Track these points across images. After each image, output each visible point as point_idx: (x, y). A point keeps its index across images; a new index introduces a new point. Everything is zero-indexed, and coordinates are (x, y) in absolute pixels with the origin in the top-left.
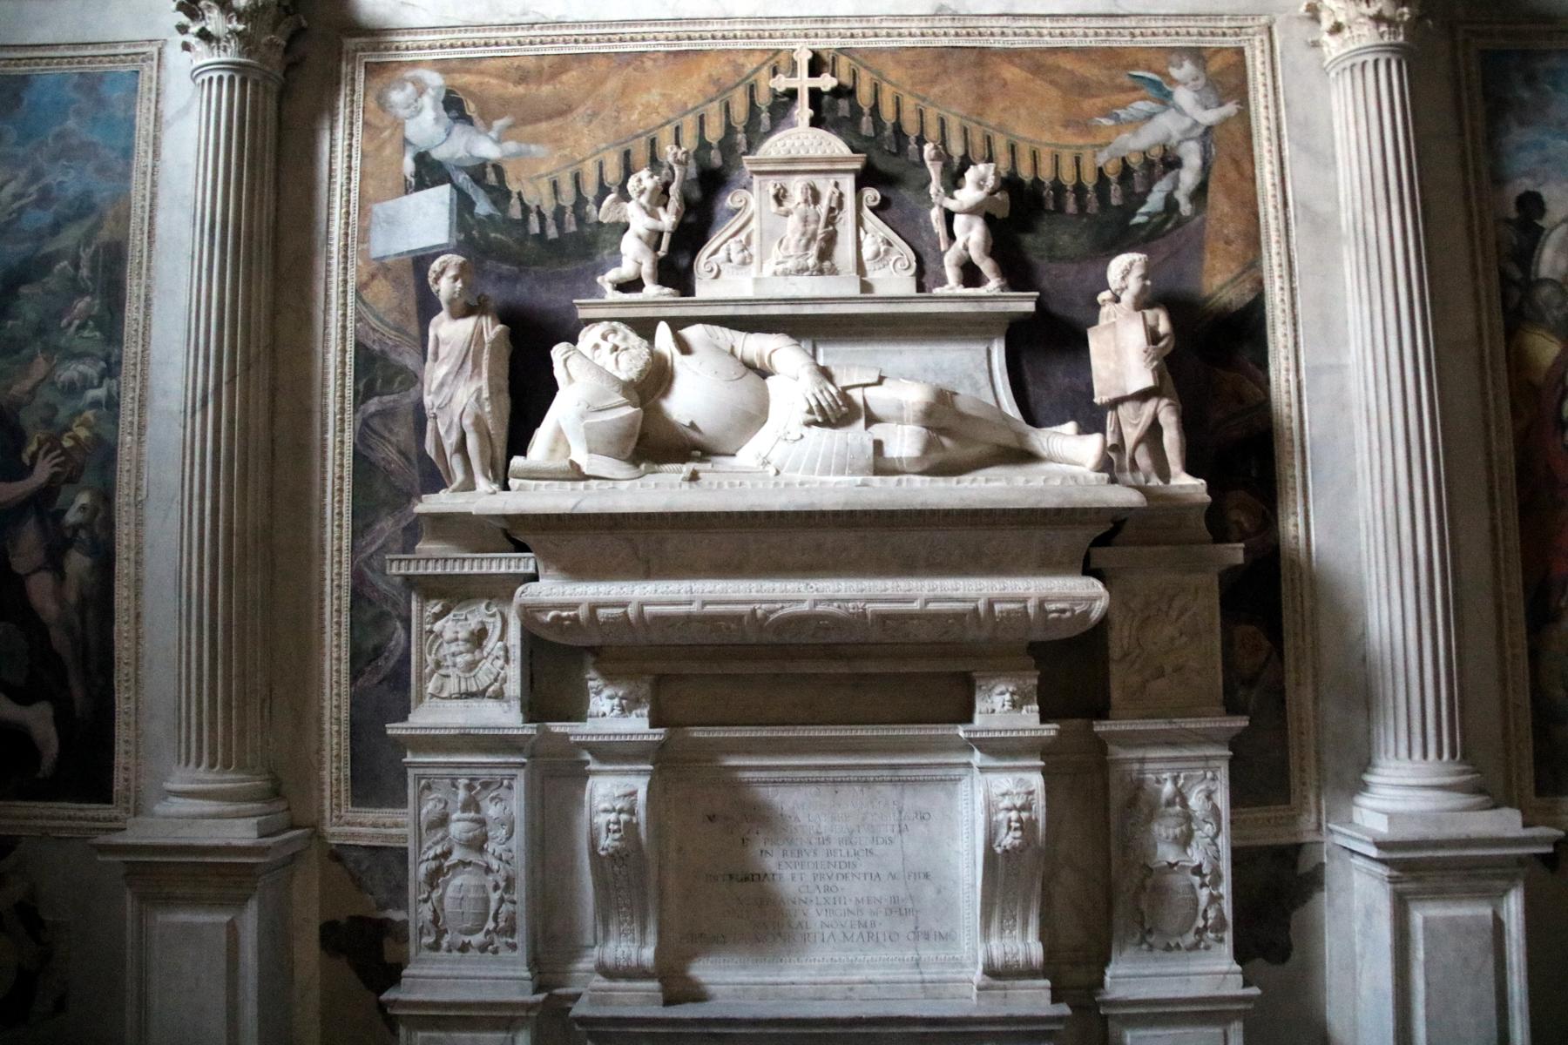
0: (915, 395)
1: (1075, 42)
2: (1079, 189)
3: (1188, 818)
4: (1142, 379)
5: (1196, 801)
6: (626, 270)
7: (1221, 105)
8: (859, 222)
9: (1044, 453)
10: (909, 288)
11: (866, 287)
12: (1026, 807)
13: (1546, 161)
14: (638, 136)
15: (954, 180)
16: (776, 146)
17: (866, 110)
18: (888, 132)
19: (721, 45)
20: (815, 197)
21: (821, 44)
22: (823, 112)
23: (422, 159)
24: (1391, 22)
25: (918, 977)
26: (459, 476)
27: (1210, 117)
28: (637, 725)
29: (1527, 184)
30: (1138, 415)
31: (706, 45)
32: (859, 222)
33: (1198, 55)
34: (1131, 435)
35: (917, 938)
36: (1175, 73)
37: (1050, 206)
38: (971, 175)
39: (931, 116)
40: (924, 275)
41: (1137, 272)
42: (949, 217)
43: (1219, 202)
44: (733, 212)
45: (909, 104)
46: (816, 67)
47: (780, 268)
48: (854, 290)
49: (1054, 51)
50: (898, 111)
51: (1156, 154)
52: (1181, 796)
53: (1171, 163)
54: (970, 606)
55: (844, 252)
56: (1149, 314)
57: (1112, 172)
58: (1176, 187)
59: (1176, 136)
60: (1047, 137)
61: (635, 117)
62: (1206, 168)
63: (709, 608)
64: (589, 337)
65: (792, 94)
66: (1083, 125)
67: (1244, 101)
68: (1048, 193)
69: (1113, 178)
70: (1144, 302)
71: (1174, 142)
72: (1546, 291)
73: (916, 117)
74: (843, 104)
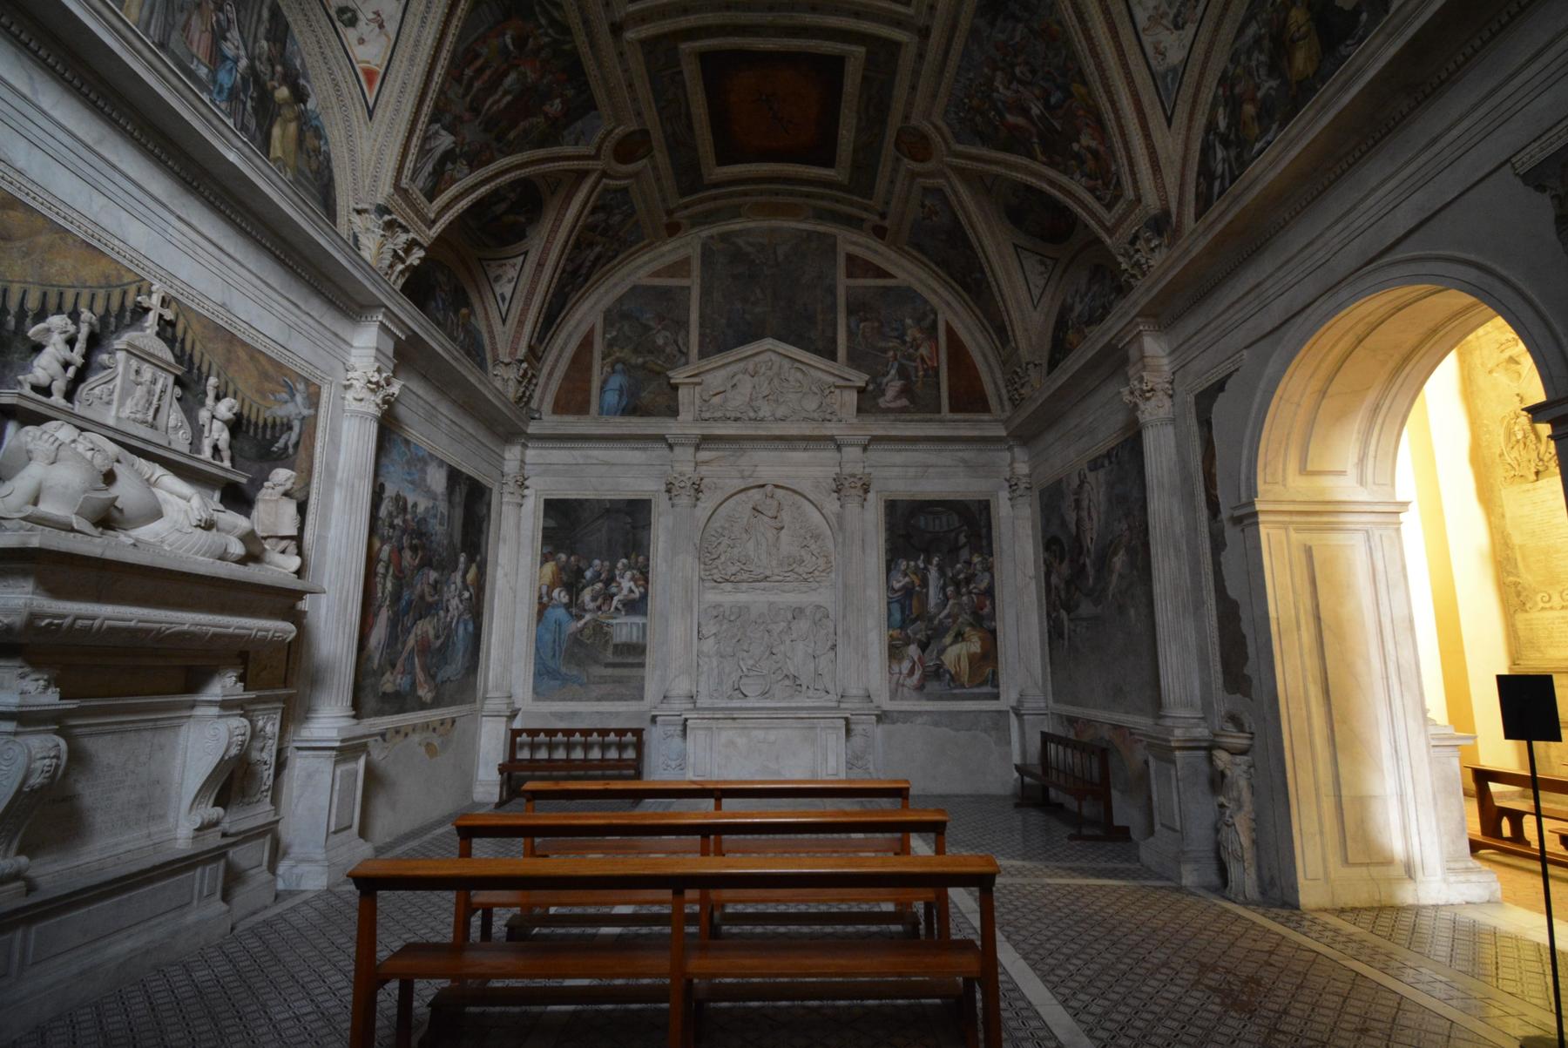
1: (269, 353)
2: (256, 424)
3: (264, 738)
5: (269, 728)
7: (309, 408)
8: (171, 405)
9: (268, 560)
10: (186, 450)
12: (244, 734)
14: (52, 286)
16: (128, 336)
17: (179, 339)
18: (186, 357)
19: (115, 256)
20: (154, 382)
22: (166, 330)
25: (151, 843)
30: (277, 545)
31: (107, 250)
32: (171, 405)
33: (307, 381)
35: (149, 821)
37: (244, 429)
39: (207, 357)
40: (195, 444)
41: (292, 480)
44: (105, 368)
45: (198, 347)
47: (133, 416)
49: (261, 352)
50: (193, 348)
51: (285, 420)
52: (263, 729)
53: (290, 428)
54: (249, 632)
57: (270, 420)
58: (288, 440)
59: (293, 416)
60: (249, 394)
61: (53, 271)
62: (300, 435)
63: (140, 625)
66: (262, 393)
67: (317, 411)
68: (245, 422)
73: (199, 354)
74: (169, 329)
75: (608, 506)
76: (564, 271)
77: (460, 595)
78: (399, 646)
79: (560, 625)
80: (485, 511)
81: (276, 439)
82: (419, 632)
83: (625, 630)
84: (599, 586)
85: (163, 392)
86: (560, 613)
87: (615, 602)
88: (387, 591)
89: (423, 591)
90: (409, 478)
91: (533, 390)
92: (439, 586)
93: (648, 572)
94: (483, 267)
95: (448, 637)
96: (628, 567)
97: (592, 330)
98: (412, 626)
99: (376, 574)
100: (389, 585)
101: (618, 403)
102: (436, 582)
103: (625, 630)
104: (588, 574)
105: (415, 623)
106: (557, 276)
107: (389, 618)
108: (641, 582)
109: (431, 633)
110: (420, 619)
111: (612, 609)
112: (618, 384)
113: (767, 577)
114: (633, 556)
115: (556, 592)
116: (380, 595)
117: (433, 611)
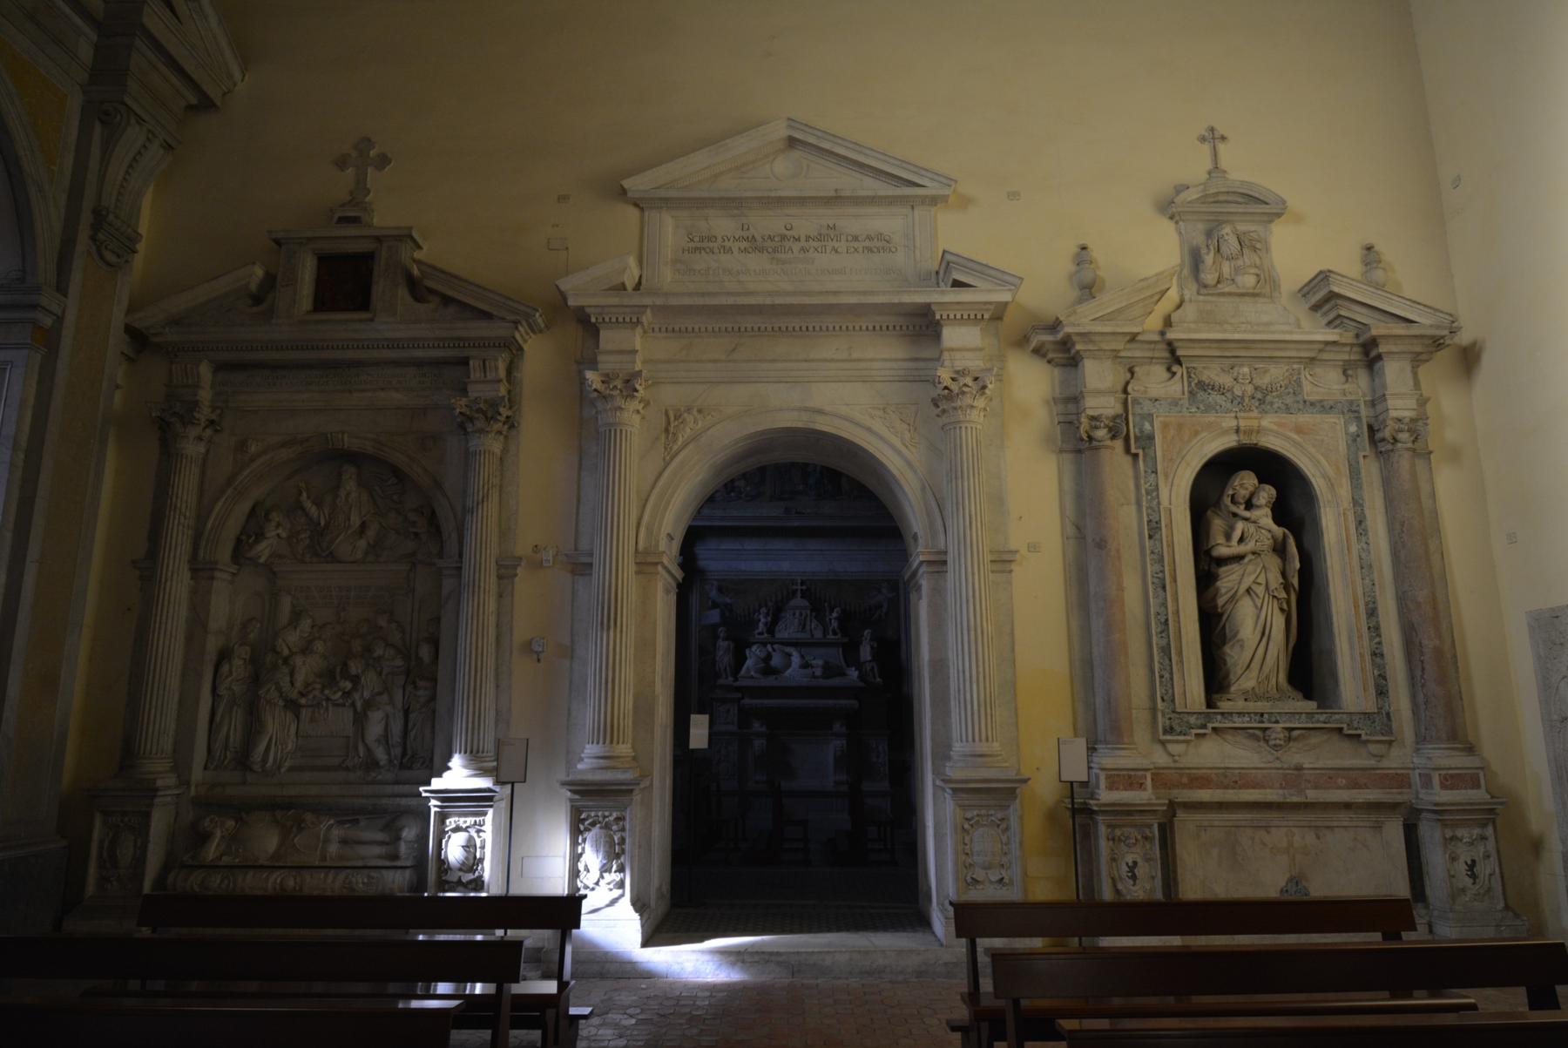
0: (820, 662)
4: (869, 658)
6: (760, 630)
11: (812, 636)
15: (832, 611)
16: (793, 603)
20: (801, 614)
21: (804, 578)
23: (713, 602)
26: (724, 676)
28: (763, 729)
34: (868, 669)
38: (835, 610)
40: (825, 632)
42: (830, 620)
46: (802, 584)
48: (809, 636)
55: (808, 628)
64: (754, 648)
65: (797, 590)
70: (871, 640)
85: (805, 618)
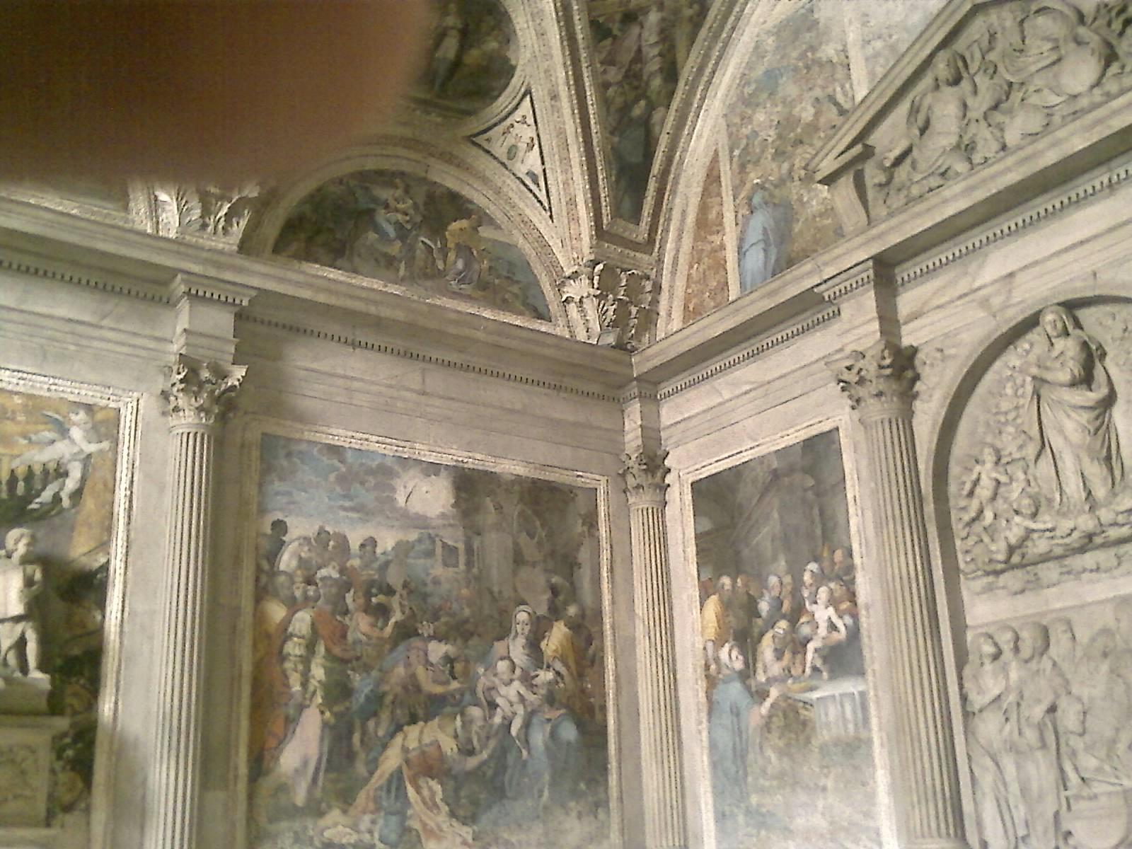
13: (293, 503)
24: (207, 412)
27: (92, 448)
29: (279, 516)
36: (73, 417)
41: (24, 541)
43: (89, 503)
51: (52, 466)
53: (62, 473)
56: (29, 568)
57: (20, 472)
58: (61, 489)
59: (67, 456)
62: (83, 479)
69: (20, 477)
71: (65, 461)
72: (282, 579)
75: (775, 465)
76: (603, 87)
77: (528, 680)
78: (361, 768)
79: (738, 715)
80: (579, 528)
81: (31, 495)
82: (413, 744)
83: (833, 711)
84: (783, 625)
86: (736, 689)
87: (810, 656)
88: (313, 683)
89: (413, 676)
90: (347, 504)
91: (655, 302)
92: (459, 667)
93: (853, 581)
94: (479, 146)
95: (502, 753)
96: (821, 578)
97: (715, 160)
98: (392, 735)
99: (282, 658)
100: (318, 672)
101: (765, 263)
102: (449, 660)
103: (833, 711)
104: (764, 607)
105: (399, 728)
106: (591, 99)
107: (325, 725)
108: (845, 605)
109: (449, 746)
110: (413, 720)
111: (808, 671)
112: (760, 231)
113: (1090, 537)
114: (825, 554)
115: (727, 646)
116: (297, 688)
117: (448, 709)
